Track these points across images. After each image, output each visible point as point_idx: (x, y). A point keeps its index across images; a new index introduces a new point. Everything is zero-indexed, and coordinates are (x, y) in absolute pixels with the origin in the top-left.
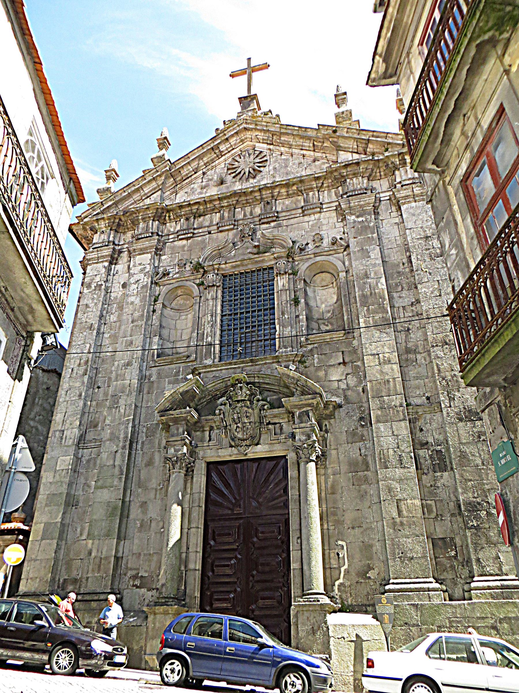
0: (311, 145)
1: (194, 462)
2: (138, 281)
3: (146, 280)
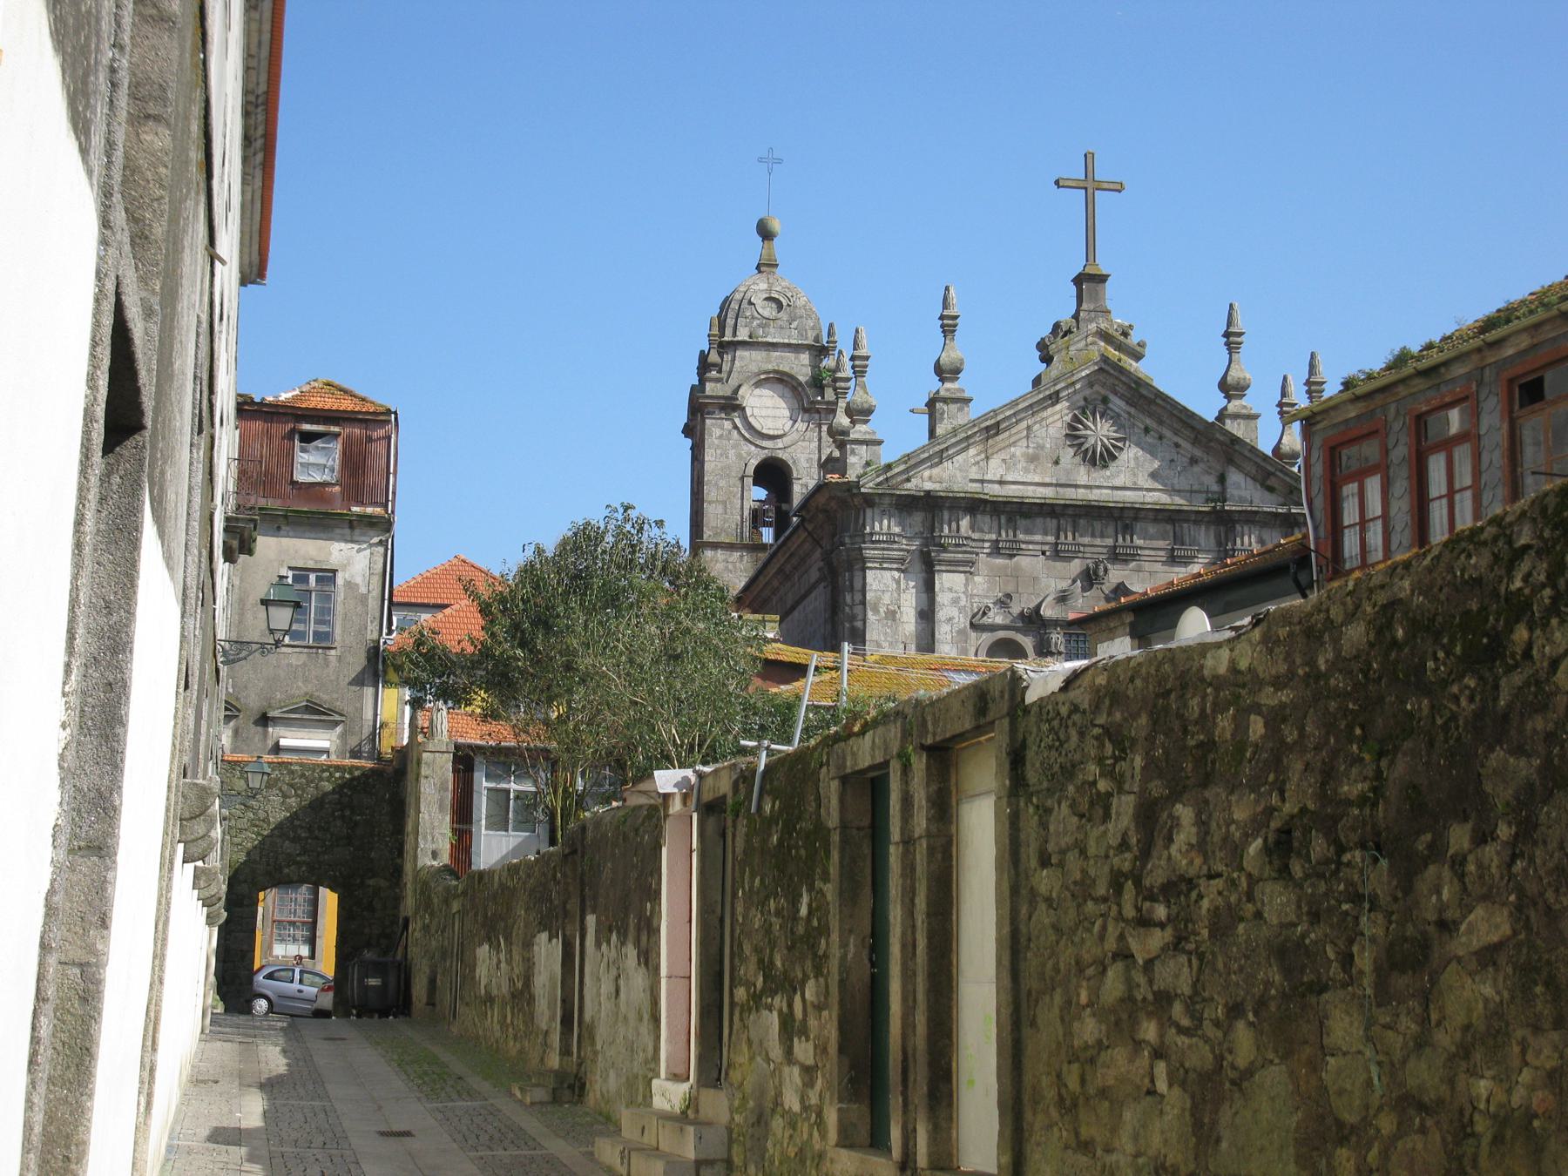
0: (1193, 436)
3: (962, 620)
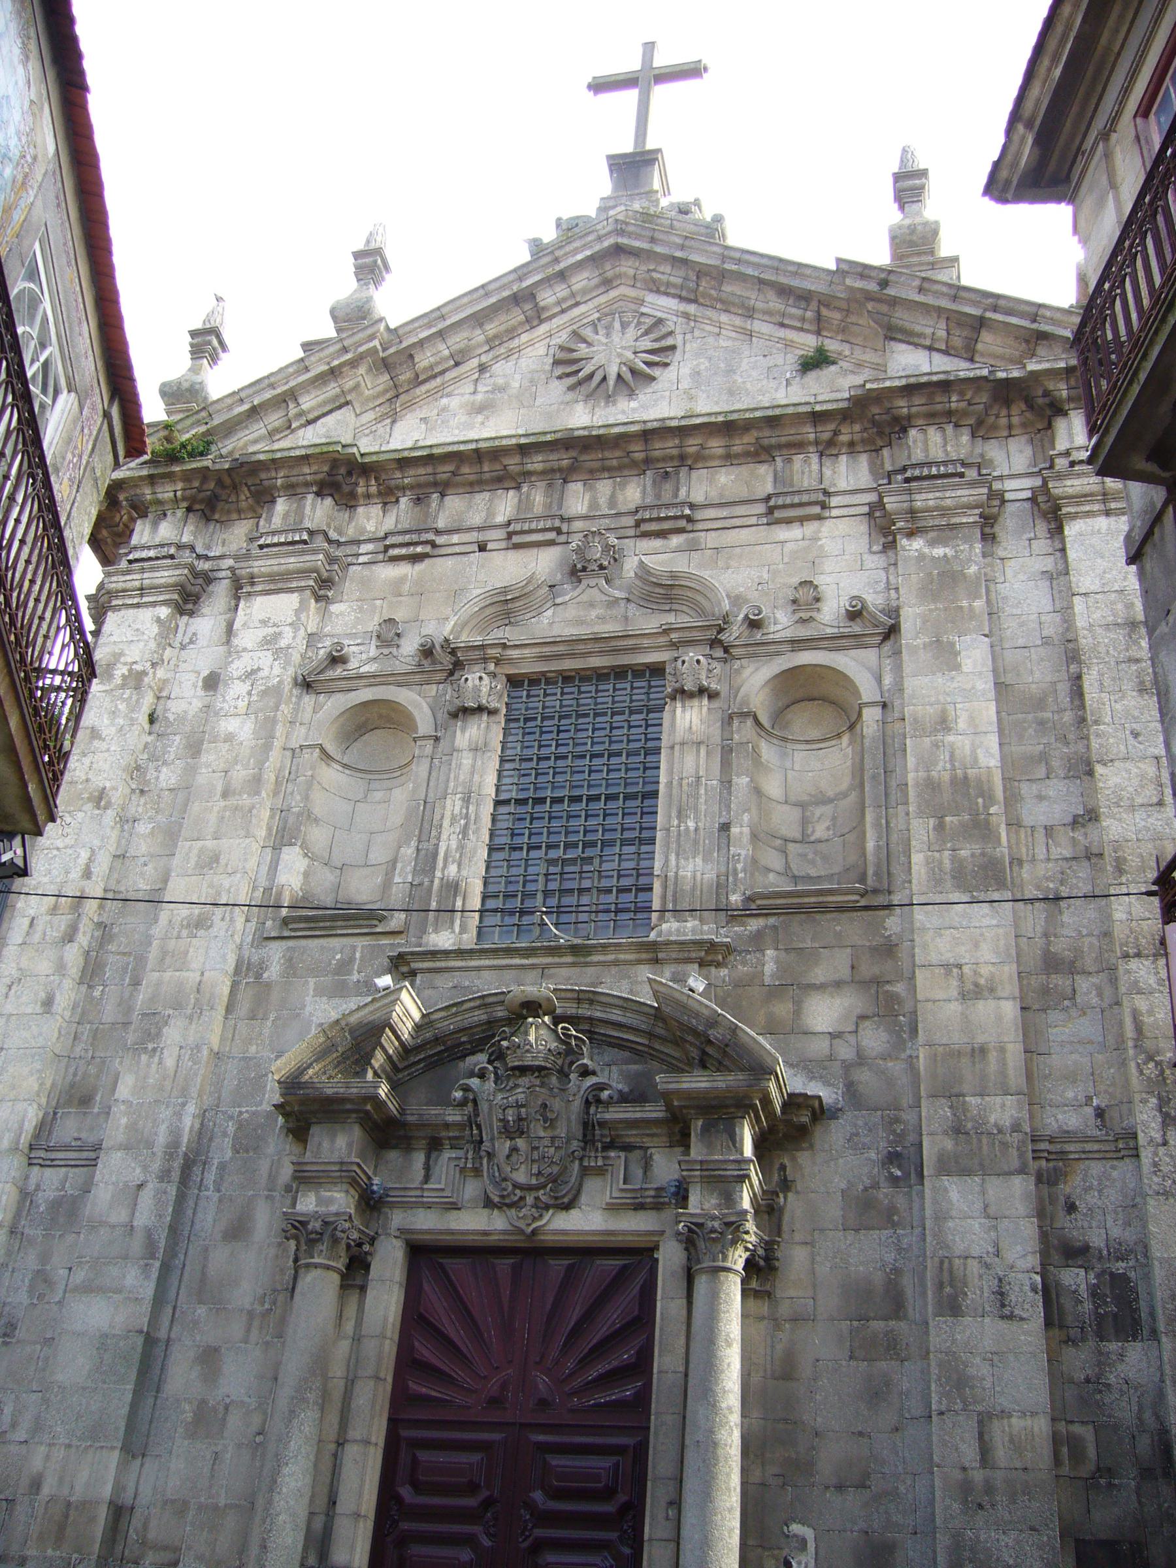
1: (372, 1241)
2: (253, 672)
3: (277, 670)
